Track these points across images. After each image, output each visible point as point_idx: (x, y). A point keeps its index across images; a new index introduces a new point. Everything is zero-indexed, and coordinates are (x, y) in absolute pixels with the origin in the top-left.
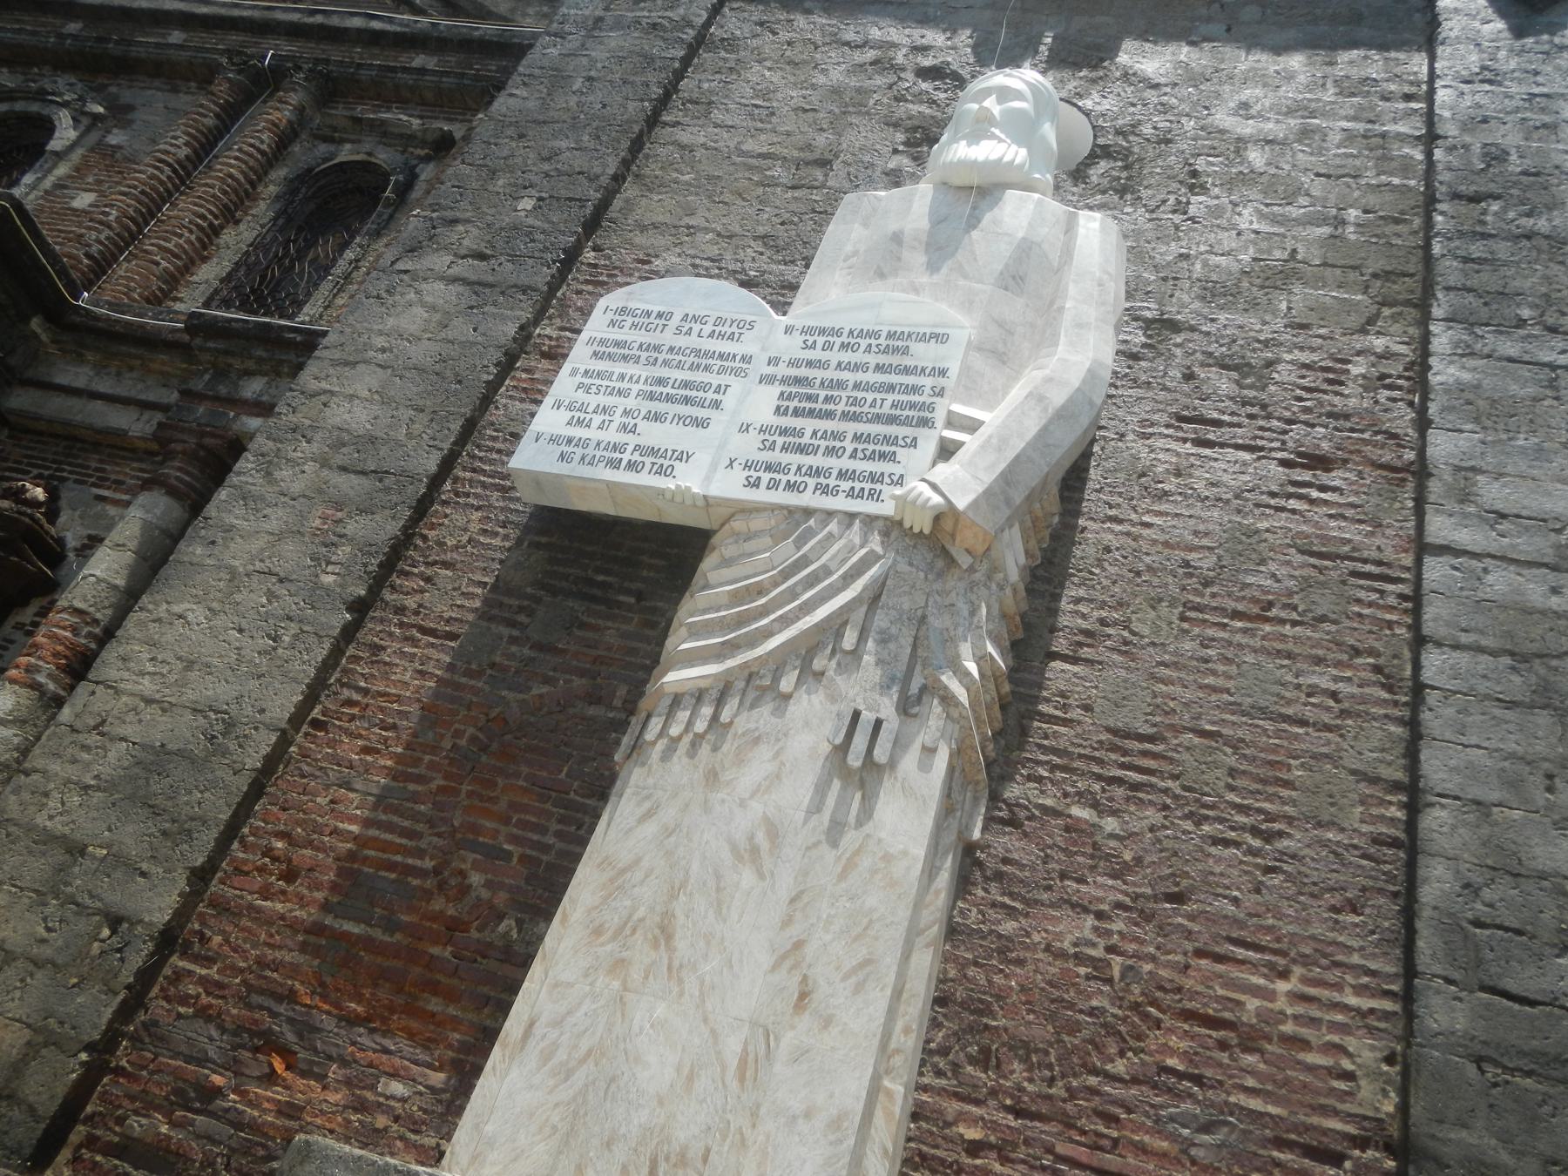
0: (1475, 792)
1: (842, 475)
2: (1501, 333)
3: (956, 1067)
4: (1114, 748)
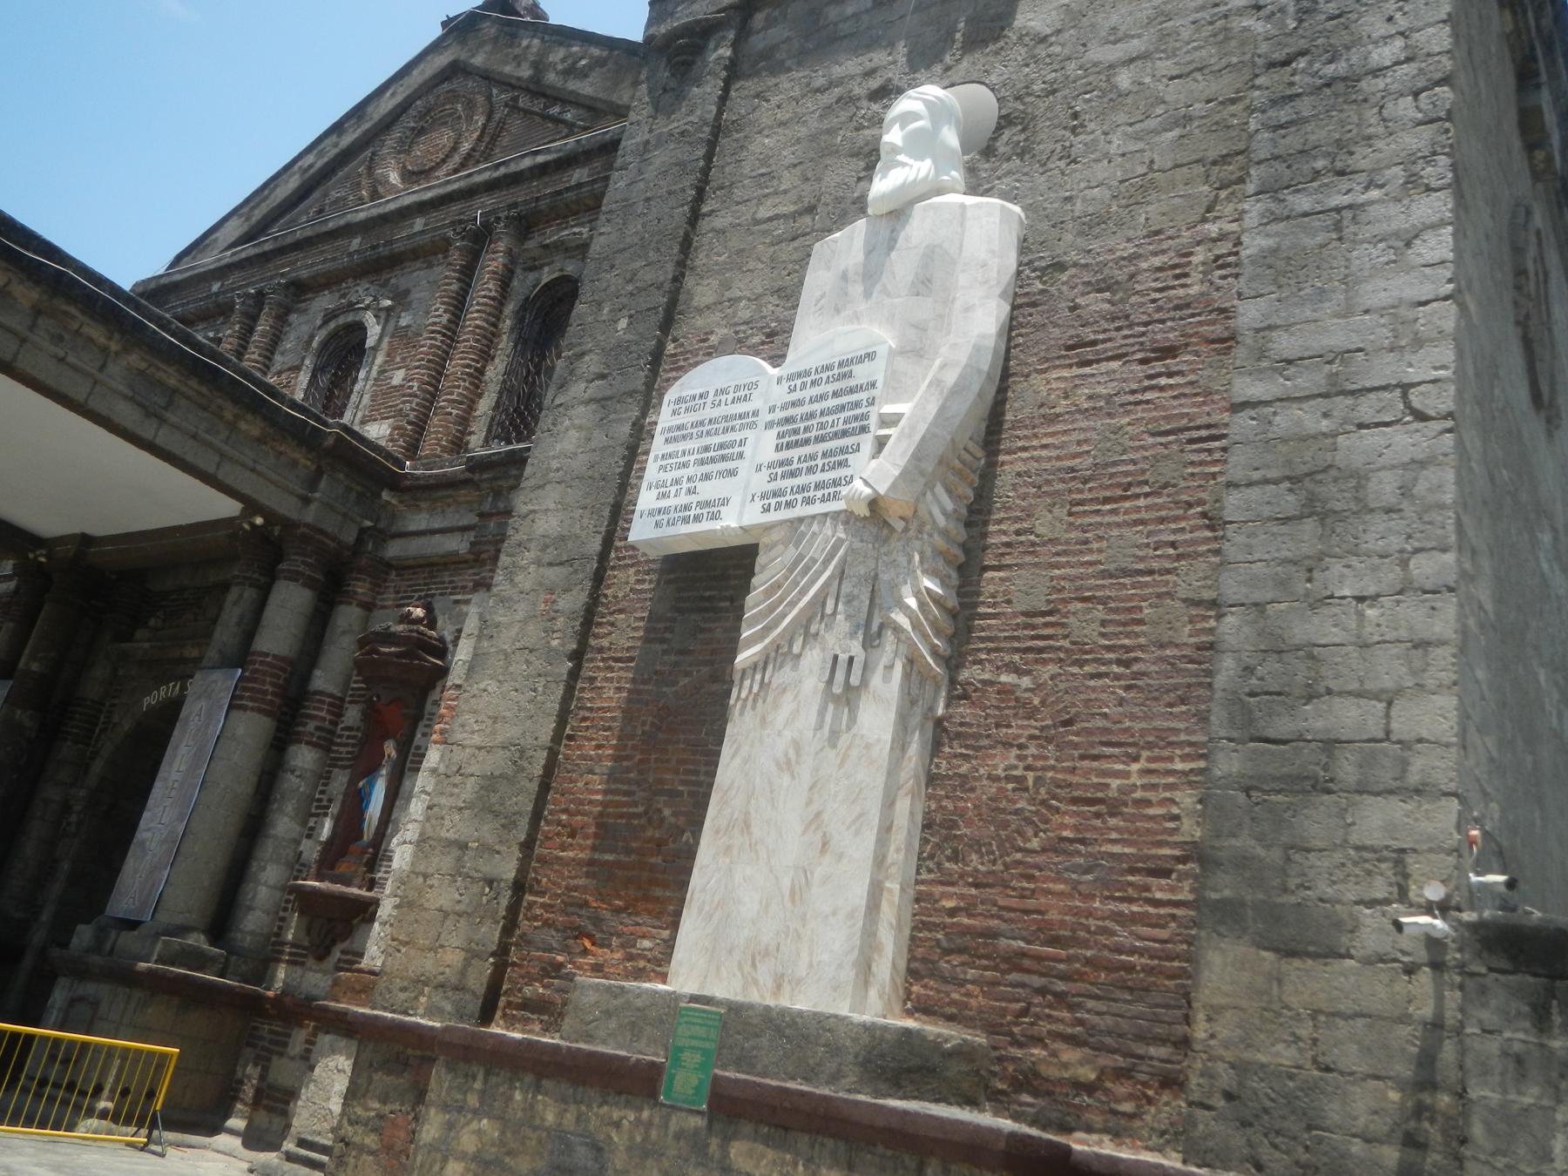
0: (1257, 596)
2: (1298, 191)
3: (939, 864)
4: (1026, 626)
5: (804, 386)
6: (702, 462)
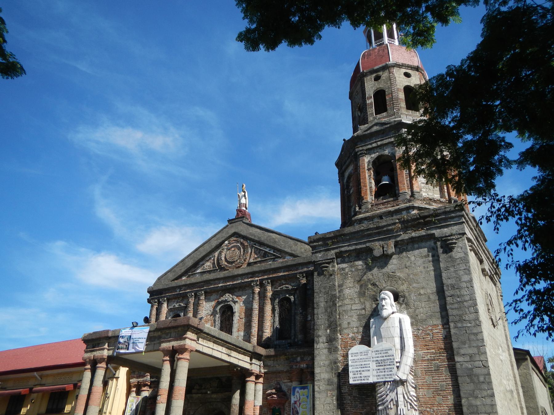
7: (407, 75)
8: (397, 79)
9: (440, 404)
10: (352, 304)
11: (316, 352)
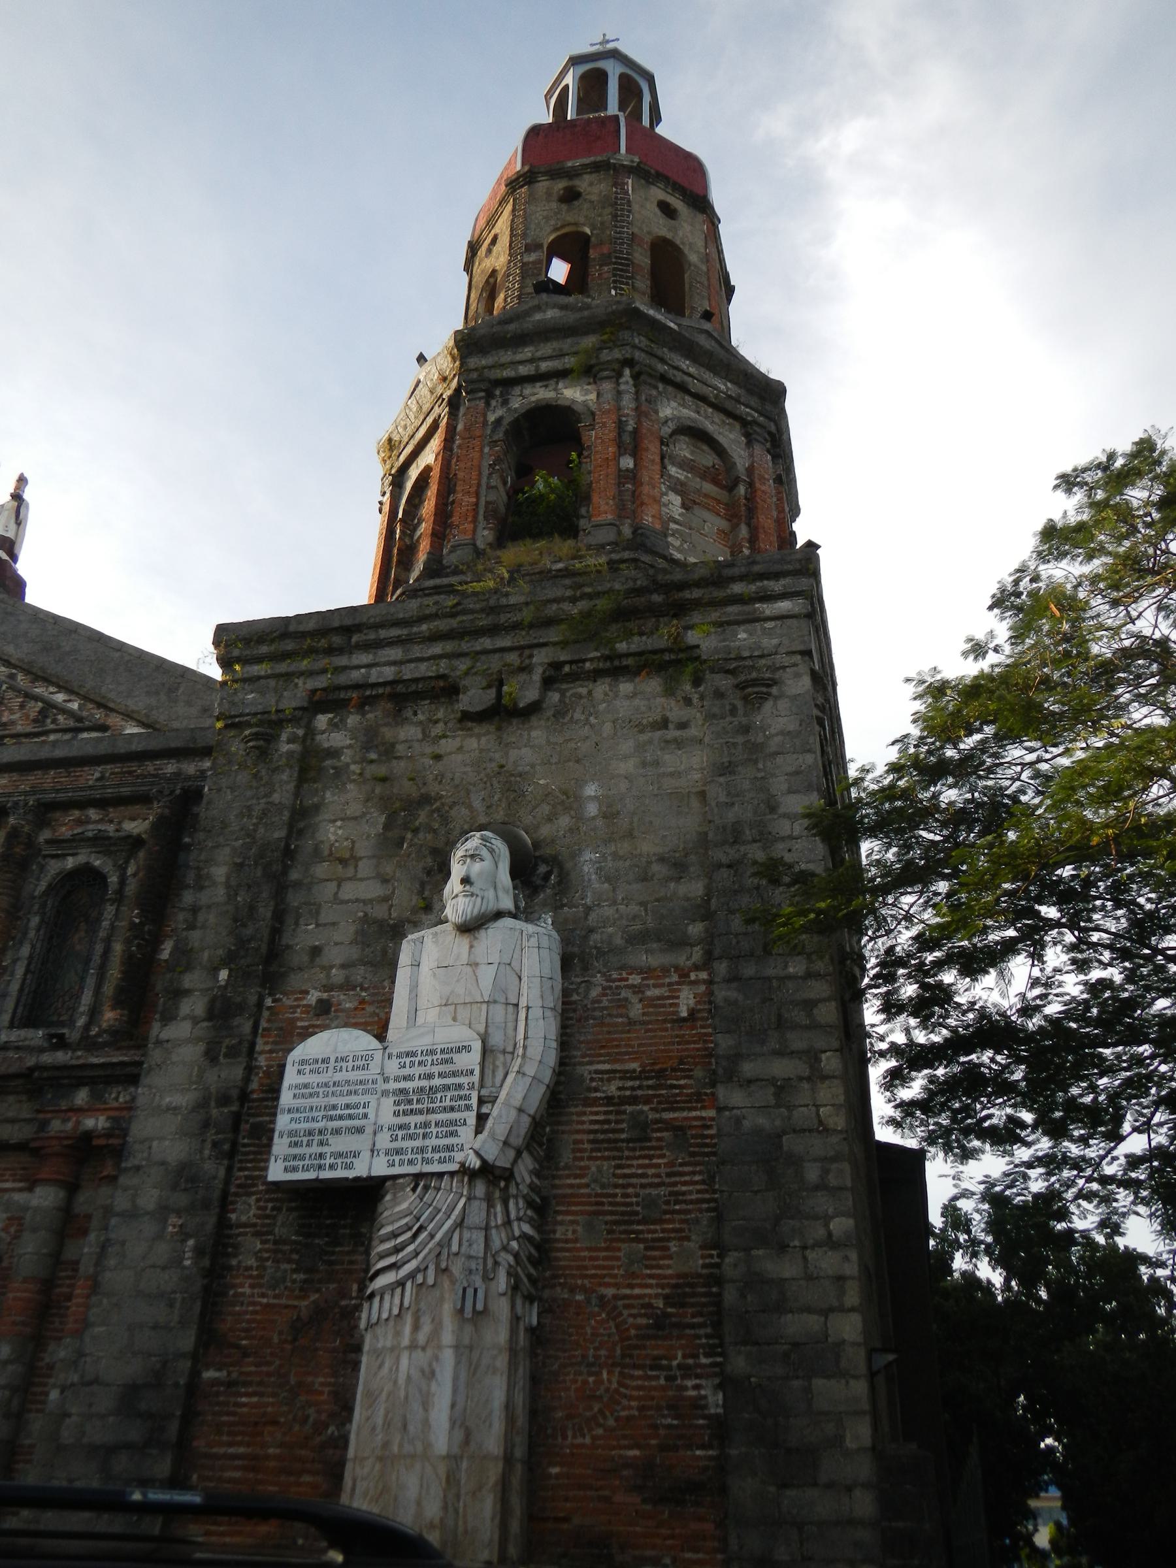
1: (435, 1149)
5: (412, 1064)
6: (331, 1118)
7: (667, 210)
8: (635, 207)
9: (633, 1275)
10: (340, 882)
11: (156, 1055)
